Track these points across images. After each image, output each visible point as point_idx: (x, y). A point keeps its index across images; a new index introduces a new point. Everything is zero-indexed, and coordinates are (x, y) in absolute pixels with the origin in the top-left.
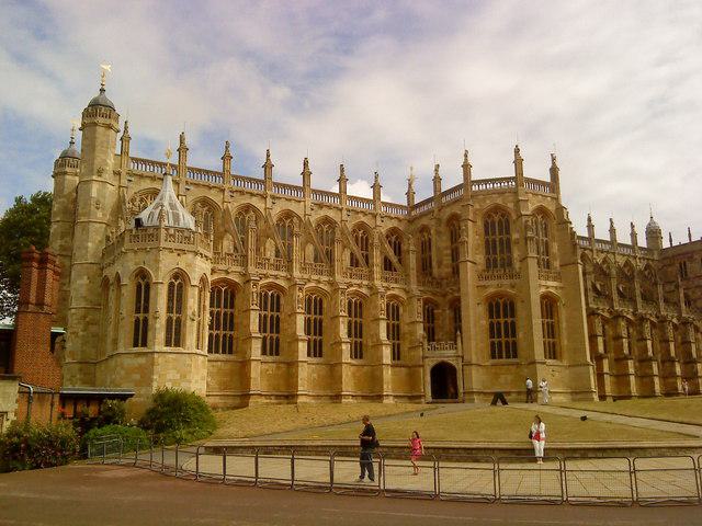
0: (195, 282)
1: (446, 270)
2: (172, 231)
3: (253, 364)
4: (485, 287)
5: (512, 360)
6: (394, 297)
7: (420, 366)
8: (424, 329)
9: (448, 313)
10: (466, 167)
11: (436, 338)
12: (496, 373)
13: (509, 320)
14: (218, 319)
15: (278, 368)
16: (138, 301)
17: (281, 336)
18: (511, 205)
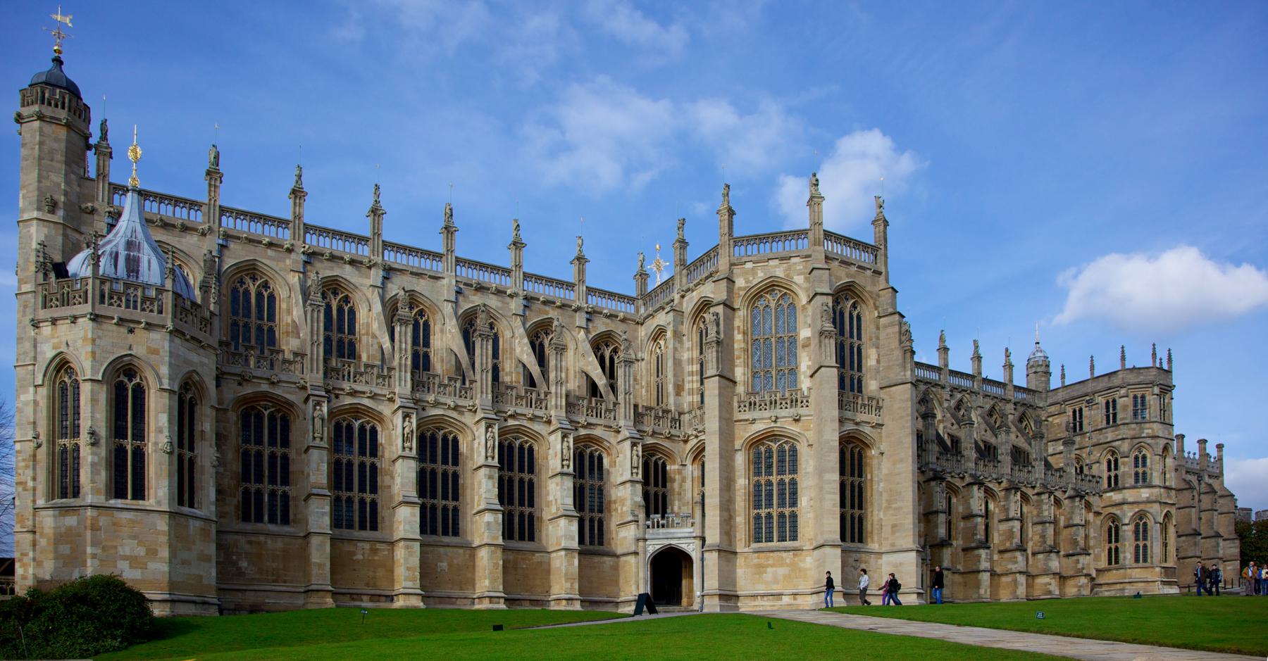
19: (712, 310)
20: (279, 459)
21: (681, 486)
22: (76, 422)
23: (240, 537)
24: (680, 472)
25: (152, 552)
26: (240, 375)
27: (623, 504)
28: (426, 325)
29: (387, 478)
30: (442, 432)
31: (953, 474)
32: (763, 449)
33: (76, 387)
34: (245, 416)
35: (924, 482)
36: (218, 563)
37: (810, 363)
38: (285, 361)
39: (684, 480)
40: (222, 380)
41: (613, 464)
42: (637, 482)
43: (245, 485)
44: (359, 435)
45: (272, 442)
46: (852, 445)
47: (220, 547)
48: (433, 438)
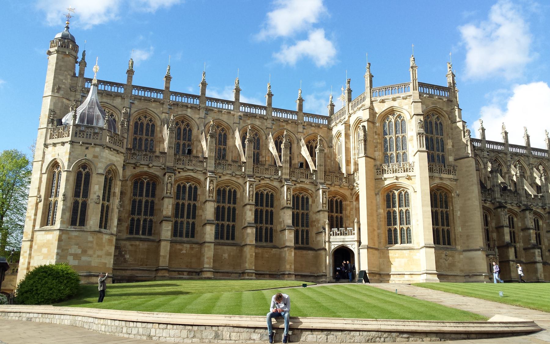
11: (344, 226)
13: (404, 209)
14: (140, 206)
15: (192, 248)
19: (362, 124)
20: (149, 203)
21: (350, 213)
22: (58, 190)
23: (127, 242)
25: (84, 252)
26: (134, 164)
28: (225, 135)
29: (200, 211)
30: (229, 188)
31: (513, 204)
33: (60, 173)
34: (135, 183)
35: (494, 209)
36: (115, 256)
38: (157, 157)
40: (126, 167)
42: (325, 211)
43: (132, 216)
44: (188, 190)
46: (440, 191)
47: (117, 248)
48: (224, 191)
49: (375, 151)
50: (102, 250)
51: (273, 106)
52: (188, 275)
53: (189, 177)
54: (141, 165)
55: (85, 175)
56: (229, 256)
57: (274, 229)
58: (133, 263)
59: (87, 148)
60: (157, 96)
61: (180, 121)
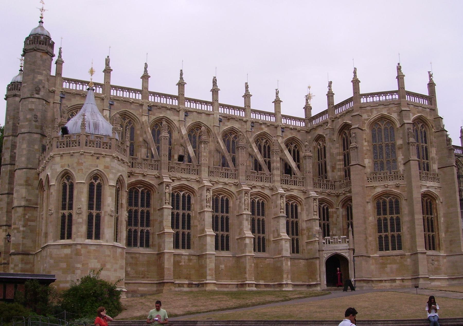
0: (113, 183)
1: (339, 173)
2: (92, 138)
3: (166, 256)
4: (374, 188)
5: (397, 252)
6: (292, 197)
7: (316, 258)
8: (320, 226)
9: (342, 212)
10: (356, 82)
11: (331, 233)
12: (383, 263)
13: (395, 216)
14: (136, 217)
15: (190, 260)
16: (64, 199)
17: (192, 232)
18: (394, 116)
21: (337, 220)
24: (336, 213)
27: (309, 231)
32: (381, 201)
37: (403, 157)
39: (338, 217)
41: (302, 210)
45: (142, 206)
49: (365, 158)
50: (117, 263)
51: (252, 107)
52: (188, 287)
53: (183, 185)
54: (136, 173)
55: (97, 186)
56: (225, 267)
57: (267, 238)
58: (135, 275)
59: (98, 158)
60: (136, 97)
61: (159, 123)
